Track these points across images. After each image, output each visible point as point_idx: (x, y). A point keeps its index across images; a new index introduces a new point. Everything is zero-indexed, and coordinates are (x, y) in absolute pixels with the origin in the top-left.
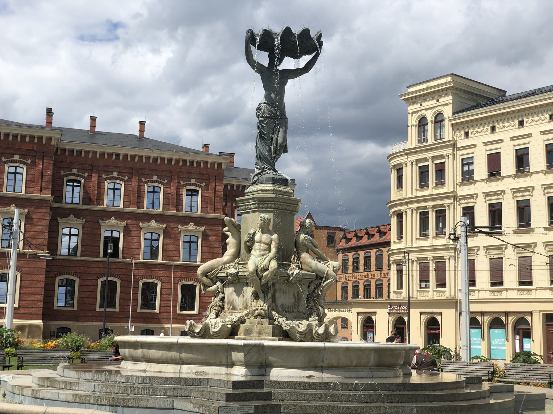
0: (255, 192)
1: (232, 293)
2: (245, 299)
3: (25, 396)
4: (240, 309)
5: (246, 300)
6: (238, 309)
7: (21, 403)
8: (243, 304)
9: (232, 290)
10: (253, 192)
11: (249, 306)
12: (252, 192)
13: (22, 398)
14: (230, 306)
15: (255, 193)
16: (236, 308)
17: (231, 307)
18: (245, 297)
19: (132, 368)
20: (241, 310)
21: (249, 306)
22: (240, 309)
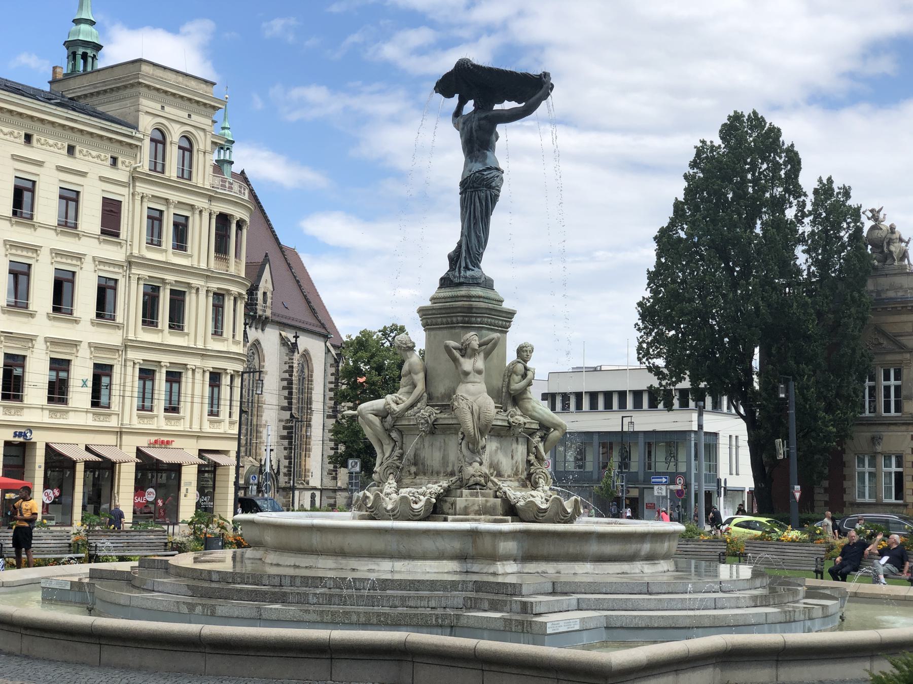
0: (495, 300)
1: (496, 451)
2: (514, 461)
3: (831, 615)
4: (509, 476)
5: (516, 462)
6: (506, 476)
7: (809, 631)
8: (512, 469)
9: (496, 447)
10: (493, 300)
11: (520, 472)
12: (490, 299)
13: (809, 624)
14: (494, 470)
15: (494, 302)
16: (503, 473)
17: (495, 472)
18: (515, 458)
19: (654, 571)
20: (509, 477)
21: (520, 472)
22: (509, 476)
